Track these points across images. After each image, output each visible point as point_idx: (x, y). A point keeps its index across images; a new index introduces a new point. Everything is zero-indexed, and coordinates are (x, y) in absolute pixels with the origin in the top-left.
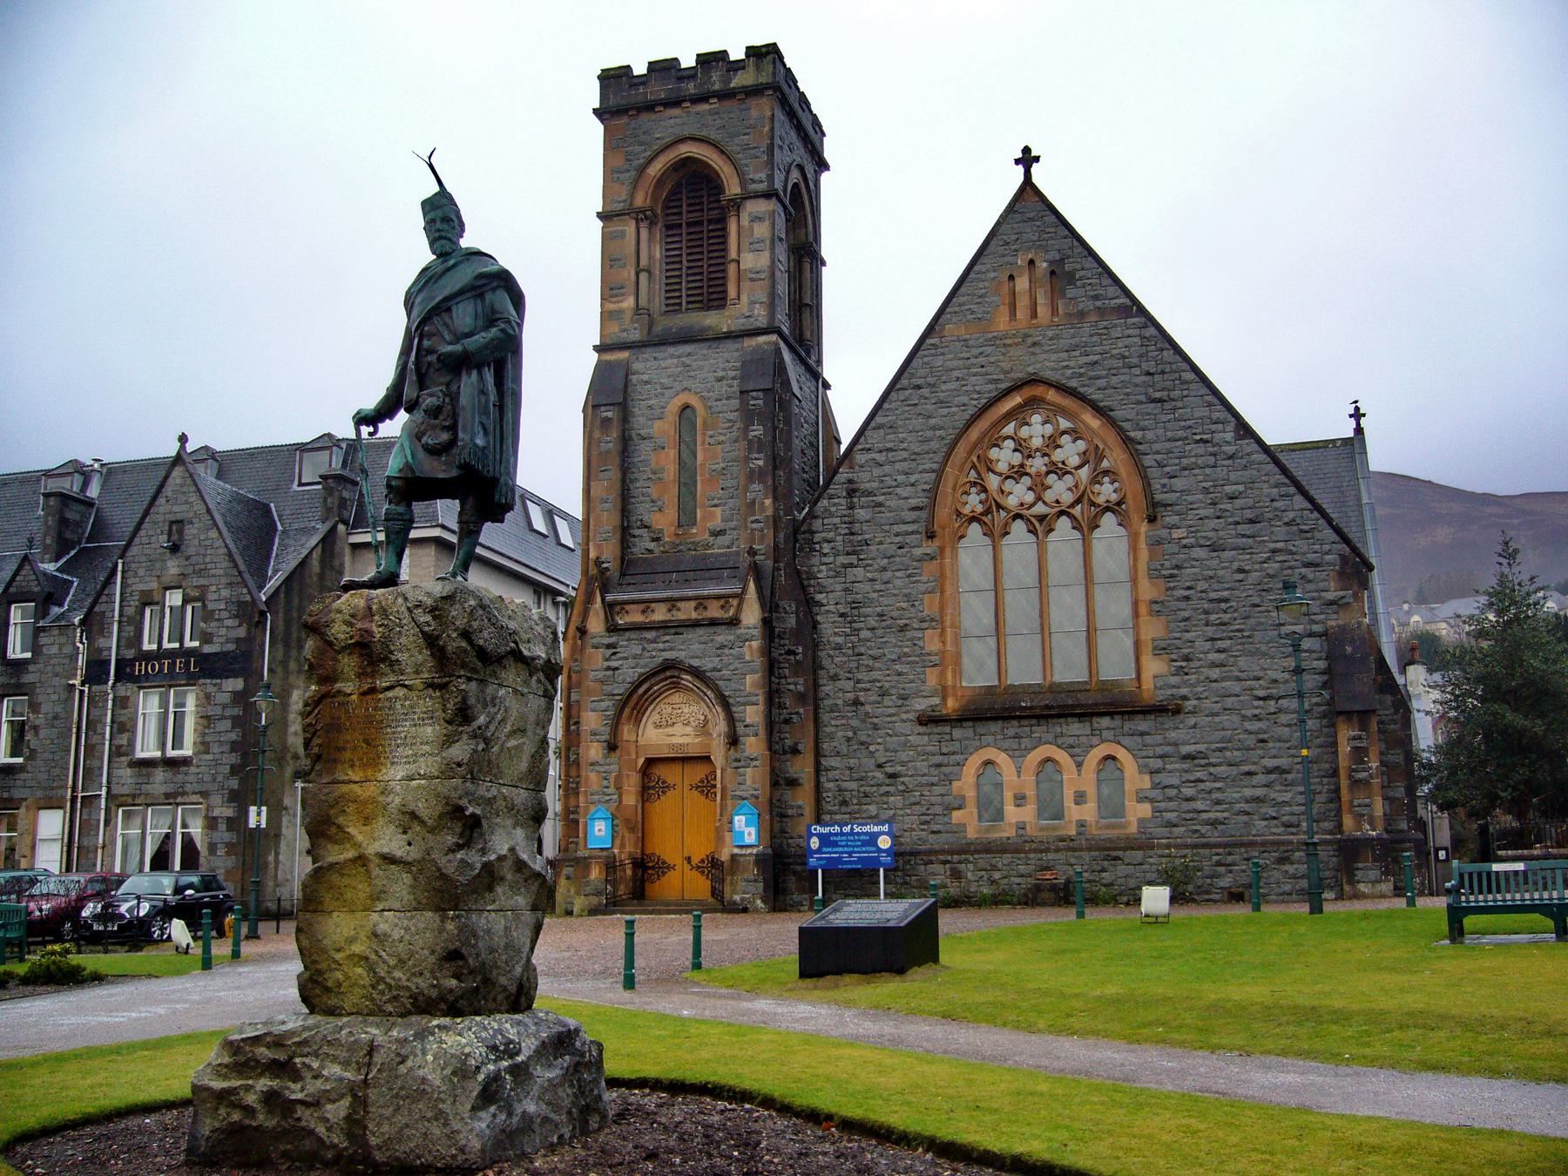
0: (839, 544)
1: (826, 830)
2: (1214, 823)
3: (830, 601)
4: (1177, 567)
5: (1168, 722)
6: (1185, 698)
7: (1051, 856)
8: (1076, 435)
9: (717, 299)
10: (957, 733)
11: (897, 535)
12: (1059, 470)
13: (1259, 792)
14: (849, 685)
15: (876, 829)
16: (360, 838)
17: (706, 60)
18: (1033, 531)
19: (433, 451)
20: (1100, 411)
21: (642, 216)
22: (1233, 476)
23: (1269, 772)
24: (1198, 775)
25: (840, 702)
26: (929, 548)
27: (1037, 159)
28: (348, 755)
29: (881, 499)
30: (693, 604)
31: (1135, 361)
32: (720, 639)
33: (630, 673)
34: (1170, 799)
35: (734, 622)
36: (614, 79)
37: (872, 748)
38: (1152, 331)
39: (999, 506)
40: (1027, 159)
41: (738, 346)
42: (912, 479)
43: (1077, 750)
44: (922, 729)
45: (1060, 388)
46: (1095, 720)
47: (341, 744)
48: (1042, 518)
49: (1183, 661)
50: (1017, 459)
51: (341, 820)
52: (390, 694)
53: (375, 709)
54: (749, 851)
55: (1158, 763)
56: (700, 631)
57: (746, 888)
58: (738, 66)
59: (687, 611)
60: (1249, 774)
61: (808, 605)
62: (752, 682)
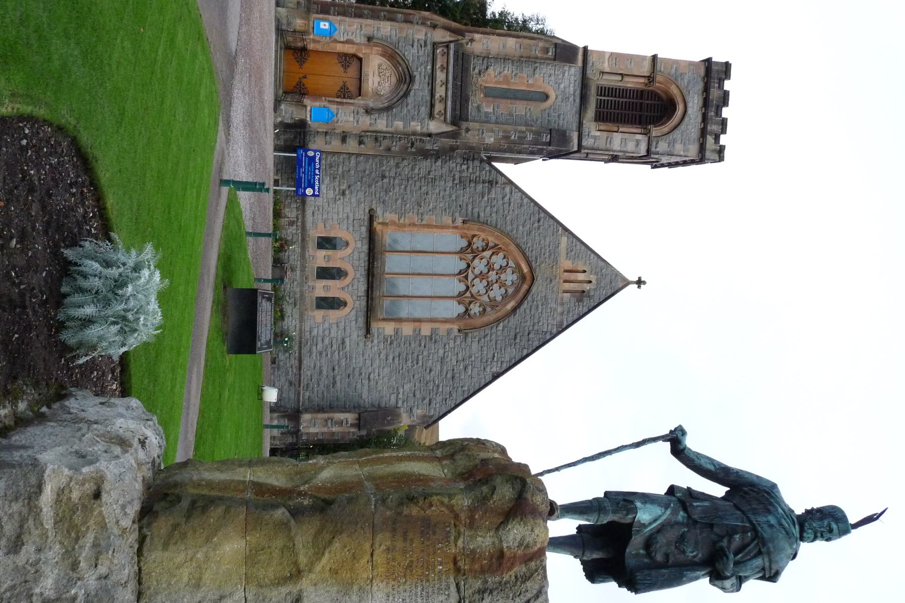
0: (465, 174)
1: (317, 161)
2: (310, 352)
3: (438, 168)
4: (435, 342)
5: (363, 332)
6: (372, 342)
7: (298, 272)
8: (505, 296)
9: (600, 117)
10: (364, 229)
11: (467, 206)
12: (489, 287)
13: (325, 372)
14: (392, 174)
15: (316, 188)
16: (318, 568)
17: (724, 123)
18: (460, 273)
19: (648, 544)
20: (514, 310)
21: (651, 79)
22: (475, 370)
23: (334, 378)
24: (334, 347)
25: (384, 168)
26: (459, 221)
27: (639, 287)
28: (400, 544)
29: (486, 199)
30: (444, 95)
31: (536, 328)
32: (423, 109)
33: (411, 54)
34: (324, 331)
35: (431, 116)
36: (726, 69)
37: (359, 183)
38: (548, 337)
39: (474, 257)
40: (640, 282)
41: (574, 128)
42: (494, 215)
43: (350, 287)
44: (367, 211)
45: (528, 291)
46: (365, 298)
47: (410, 535)
48: (466, 277)
49: (390, 341)
50: (497, 267)
51: (337, 545)
52: (453, 588)
53: (440, 571)
54: (308, 116)
55: (342, 327)
56: (428, 98)
57: (289, 112)
58: (717, 138)
59: (440, 92)
60: (334, 369)
61: (437, 155)
62: (399, 125)
